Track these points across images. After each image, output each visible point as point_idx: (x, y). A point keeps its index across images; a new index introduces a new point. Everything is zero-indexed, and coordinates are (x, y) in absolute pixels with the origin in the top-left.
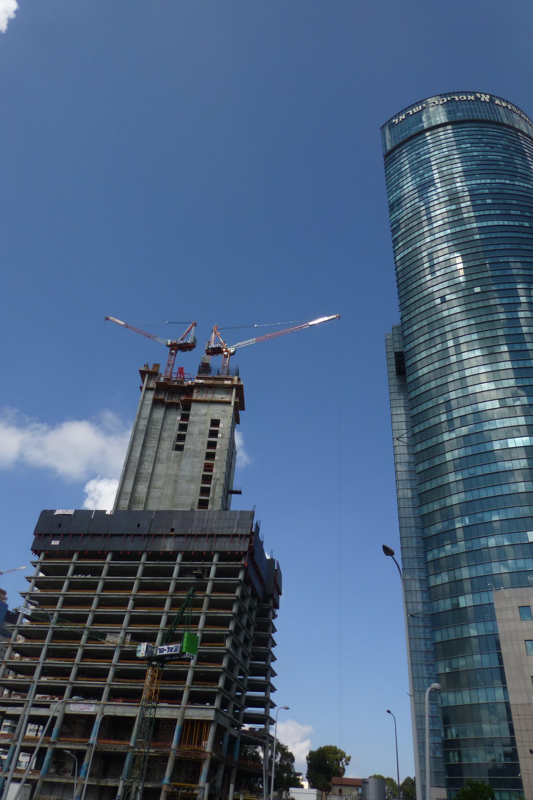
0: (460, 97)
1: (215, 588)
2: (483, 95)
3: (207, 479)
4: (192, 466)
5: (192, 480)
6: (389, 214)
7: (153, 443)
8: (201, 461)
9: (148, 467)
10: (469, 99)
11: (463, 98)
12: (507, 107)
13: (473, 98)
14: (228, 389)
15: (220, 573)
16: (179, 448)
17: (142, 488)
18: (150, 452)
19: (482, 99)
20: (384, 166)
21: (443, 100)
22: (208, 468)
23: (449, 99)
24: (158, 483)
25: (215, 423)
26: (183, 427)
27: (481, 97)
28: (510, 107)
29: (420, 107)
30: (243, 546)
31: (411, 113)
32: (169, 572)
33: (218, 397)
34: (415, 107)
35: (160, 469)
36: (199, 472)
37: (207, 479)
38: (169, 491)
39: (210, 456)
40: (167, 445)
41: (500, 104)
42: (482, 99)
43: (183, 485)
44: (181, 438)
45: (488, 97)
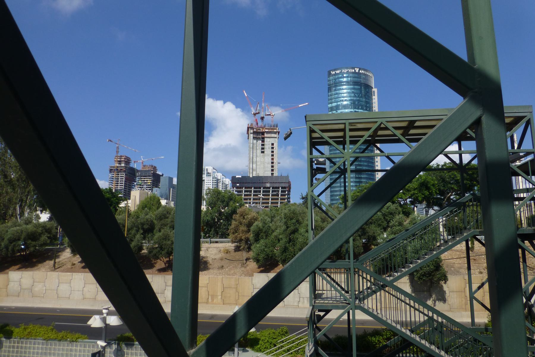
1: (281, 195)
3: (272, 163)
4: (268, 159)
5: (268, 163)
7: (255, 151)
8: (270, 157)
9: (254, 159)
13: (353, 71)
14: (275, 133)
15: (282, 192)
16: (263, 152)
17: (254, 166)
18: (254, 154)
22: (273, 159)
24: (258, 164)
25: (273, 144)
26: (263, 145)
30: (287, 185)
32: (269, 191)
33: (273, 135)
35: (258, 159)
36: (270, 161)
37: (272, 163)
38: (262, 166)
39: (273, 155)
40: (259, 151)
43: (266, 165)
44: (263, 149)
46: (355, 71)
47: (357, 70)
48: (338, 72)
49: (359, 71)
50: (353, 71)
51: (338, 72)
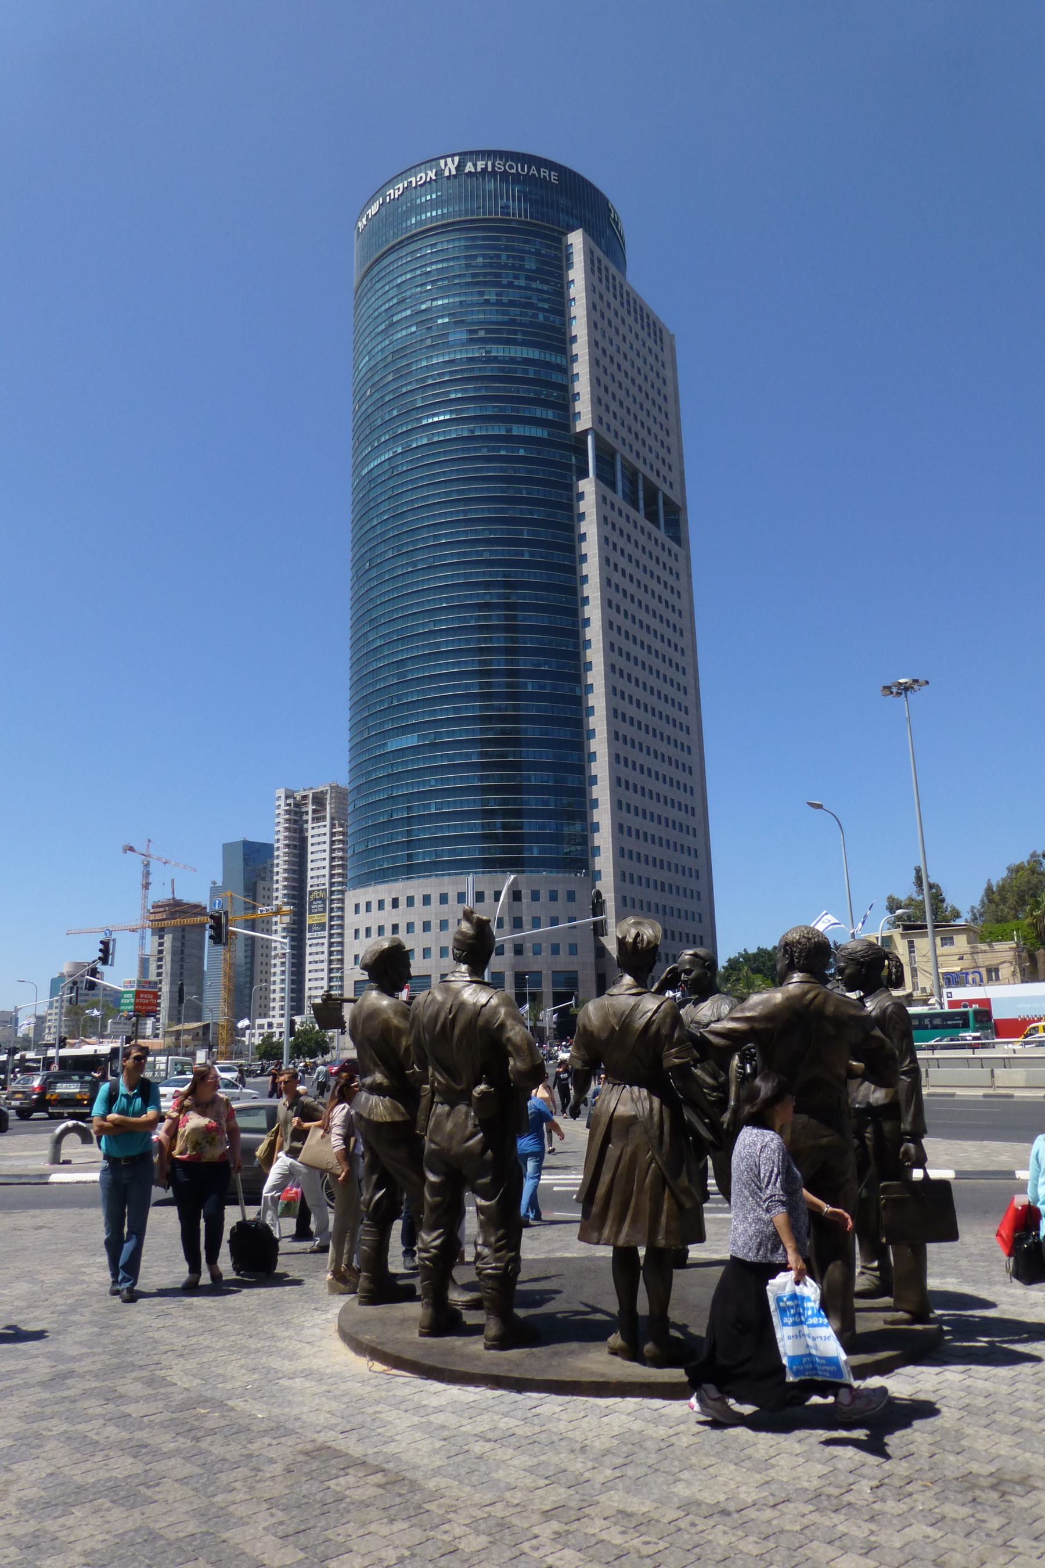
2: (449, 160)
12: (484, 170)
13: (432, 175)
19: (447, 174)
28: (490, 169)
42: (447, 174)
45: (456, 159)
46: (439, 173)
47: (450, 166)
48: (374, 209)
49: (460, 167)
50: (432, 175)
51: (374, 209)
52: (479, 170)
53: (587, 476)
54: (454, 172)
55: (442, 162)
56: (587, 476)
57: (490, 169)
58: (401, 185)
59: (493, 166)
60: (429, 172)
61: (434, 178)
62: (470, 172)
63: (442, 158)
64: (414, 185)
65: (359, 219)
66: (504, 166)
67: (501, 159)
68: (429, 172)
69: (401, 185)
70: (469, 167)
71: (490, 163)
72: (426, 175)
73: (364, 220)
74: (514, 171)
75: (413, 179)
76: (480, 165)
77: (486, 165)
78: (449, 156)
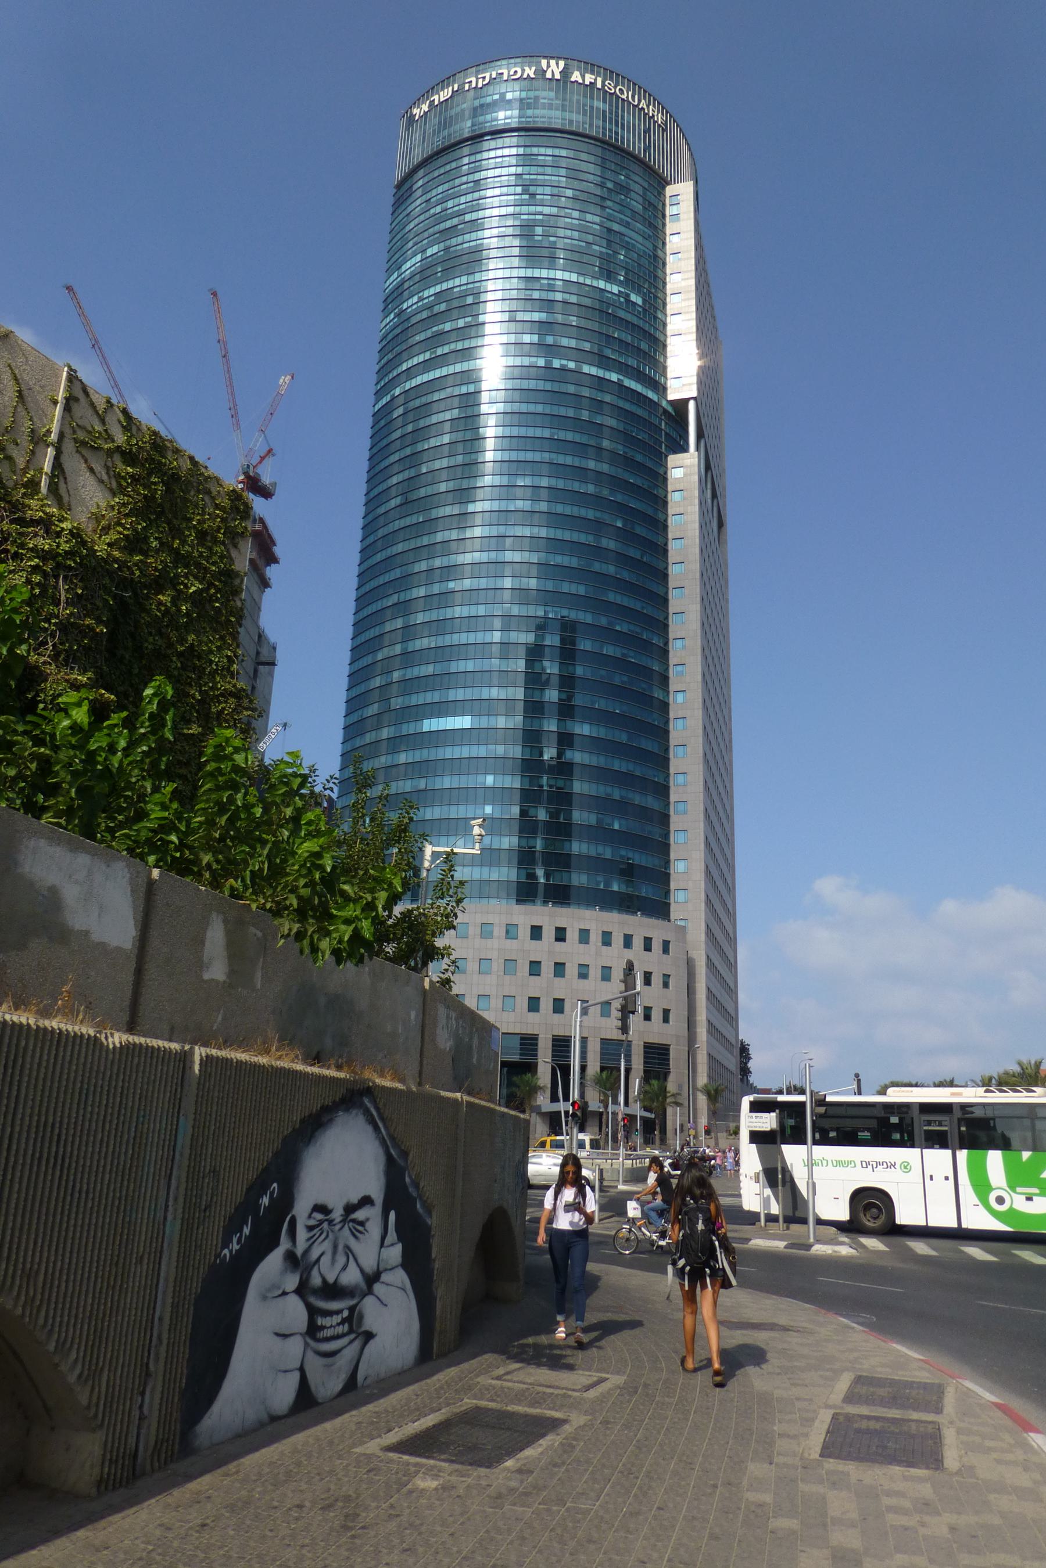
0: (512, 73)
2: (553, 62)
6: (381, 315)
10: (525, 76)
11: (516, 72)
13: (530, 72)
19: (549, 75)
20: (391, 210)
21: (484, 78)
23: (494, 76)
27: (548, 66)
28: (599, 85)
29: (450, 89)
31: (436, 103)
34: (443, 89)
41: (580, 81)
42: (549, 75)
45: (562, 63)
48: (445, 94)
49: (566, 73)
51: (445, 94)
52: (587, 83)
53: (684, 449)
54: (558, 76)
55: (544, 62)
56: (684, 449)
57: (599, 85)
58: (487, 75)
59: (603, 85)
60: (527, 69)
61: (532, 76)
62: (576, 81)
63: (545, 57)
64: (505, 77)
65: (417, 102)
66: (615, 87)
67: (611, 79)
68: (527, 69)
69: (487, 75)
70: (576, 76)
71: (599, 80)
72: (523, 71)
73: (425, 108)
74: (624, 97)
75: (505, 72)
76: (589, 78)
77: (596, 80)
78: (552, 58)
